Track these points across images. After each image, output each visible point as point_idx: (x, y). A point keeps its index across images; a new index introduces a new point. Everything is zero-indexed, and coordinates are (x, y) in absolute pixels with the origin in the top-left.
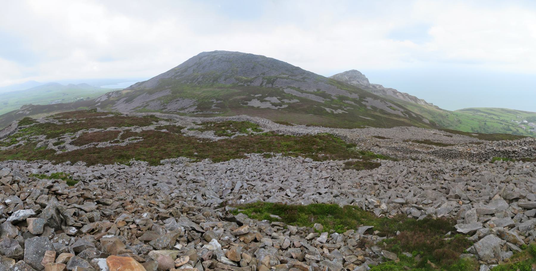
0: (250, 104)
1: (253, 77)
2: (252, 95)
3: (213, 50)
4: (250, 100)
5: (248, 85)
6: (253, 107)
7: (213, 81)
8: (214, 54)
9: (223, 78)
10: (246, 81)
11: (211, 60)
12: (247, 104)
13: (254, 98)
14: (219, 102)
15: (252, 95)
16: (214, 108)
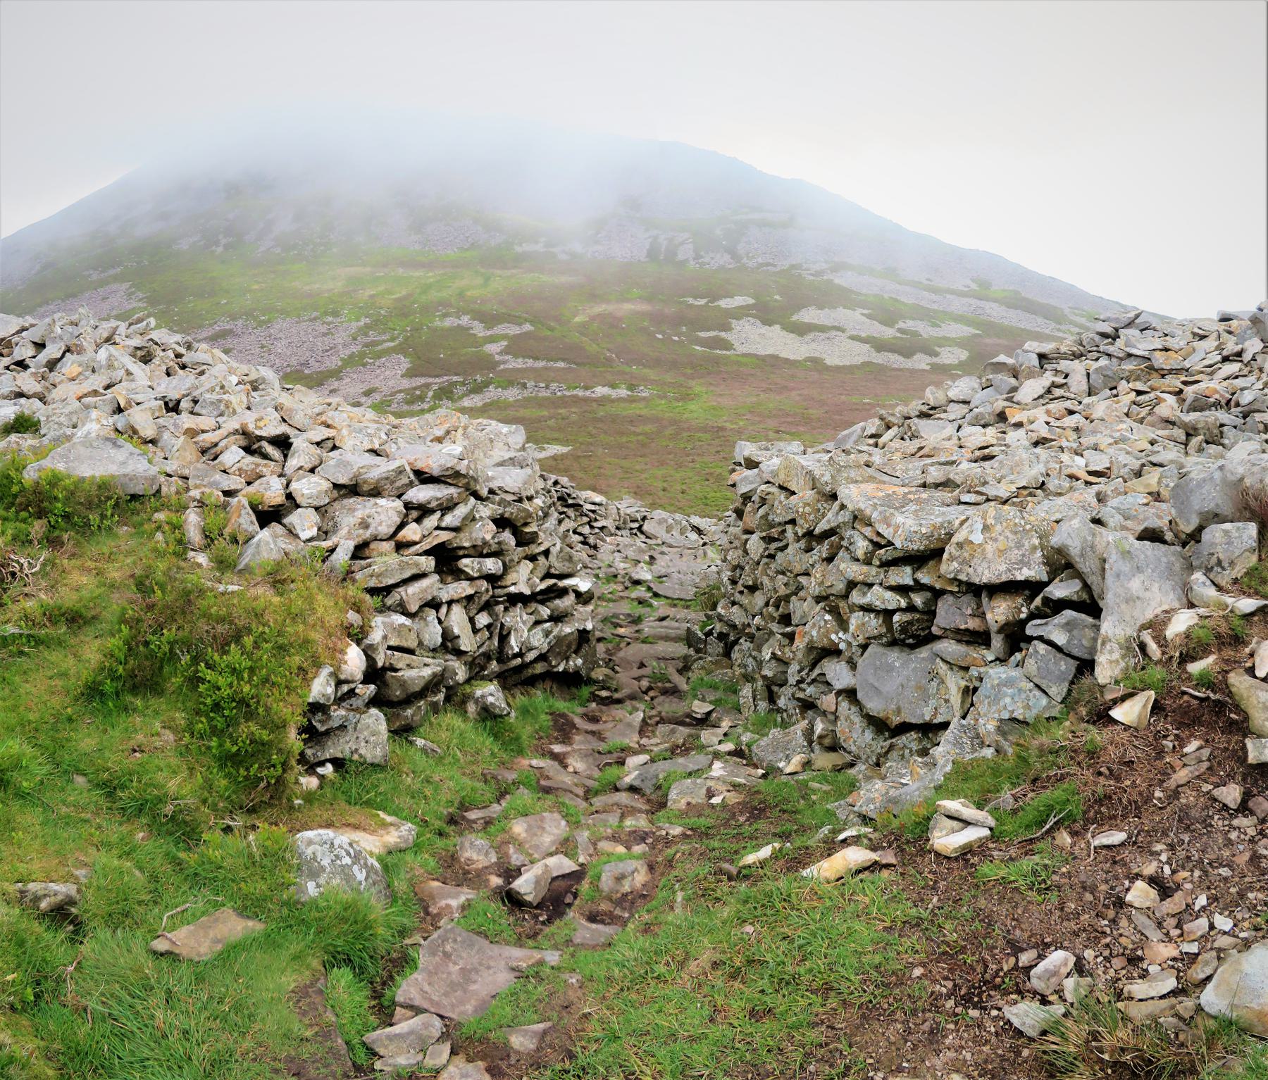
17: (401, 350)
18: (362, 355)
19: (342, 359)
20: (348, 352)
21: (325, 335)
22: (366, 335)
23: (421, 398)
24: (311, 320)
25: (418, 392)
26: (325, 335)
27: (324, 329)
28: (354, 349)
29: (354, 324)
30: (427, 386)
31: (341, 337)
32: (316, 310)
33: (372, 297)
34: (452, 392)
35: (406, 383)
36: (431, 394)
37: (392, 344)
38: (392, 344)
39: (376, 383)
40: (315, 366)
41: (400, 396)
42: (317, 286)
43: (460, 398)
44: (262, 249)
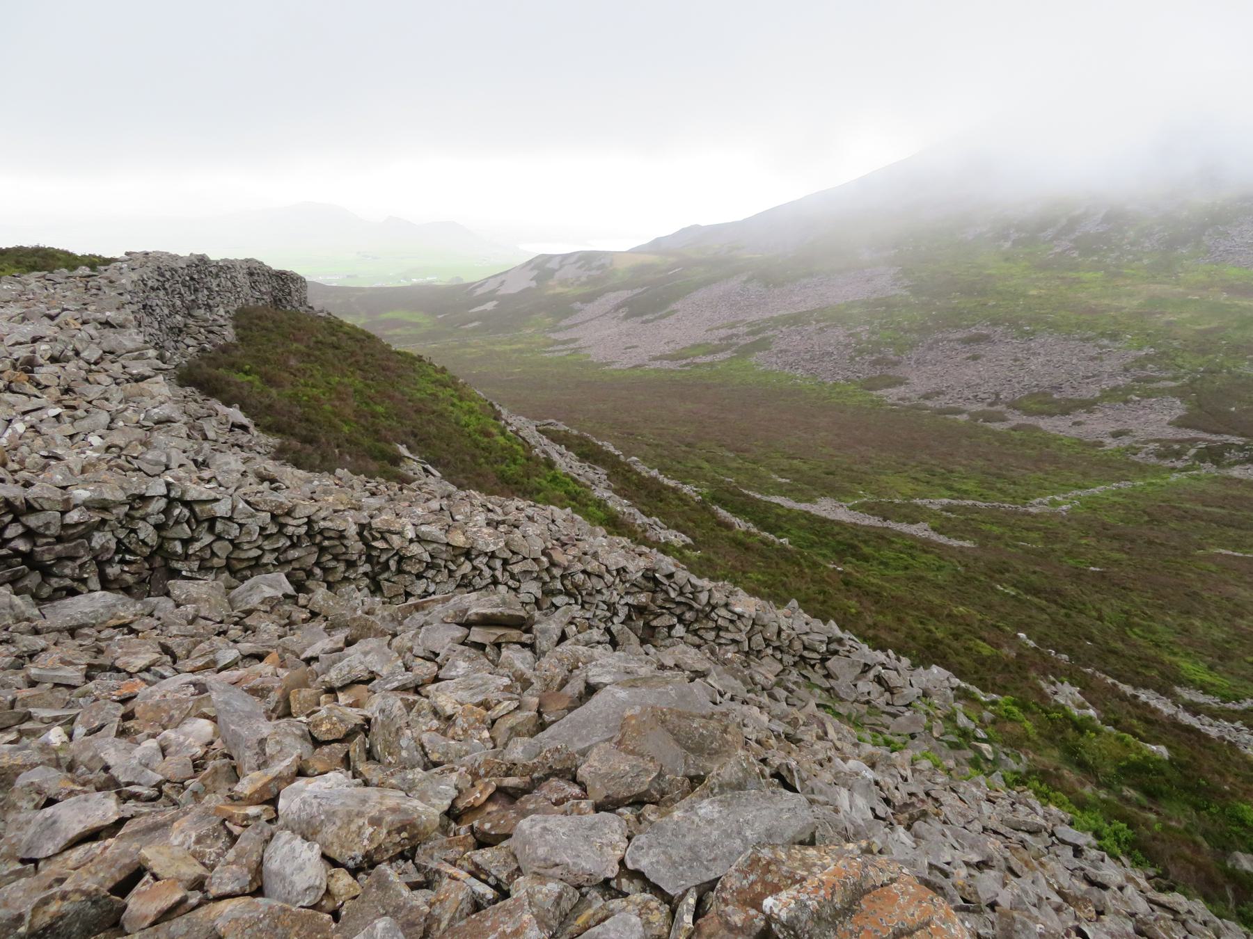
17: (1180, 393)
18: (1129, 390)
19: (1103, 390)
20: (1112, 383)
21: (1092, 359)
22: (1143, 367)
23: (1178, 455)
24: (1081, 340)
25: (1177, 447)
26: (1092, 359)
27: (1094, 353)
28: (1120, 381)
29: (1133, 352)
30: (1193, 441)
31: (1109, 365)
32: (1092, 329)
33: (1169, 323)
34: (1222, 455)
35: (1170, 433)
36: (1193, 451)
37: (1173, 384)
38: (1173, 384)
39: (1133, 425)
40: (1068, 393)
41: (1152, 446)
42: (1106, 302)
43: (1231, 465)
44: (1058, 250)
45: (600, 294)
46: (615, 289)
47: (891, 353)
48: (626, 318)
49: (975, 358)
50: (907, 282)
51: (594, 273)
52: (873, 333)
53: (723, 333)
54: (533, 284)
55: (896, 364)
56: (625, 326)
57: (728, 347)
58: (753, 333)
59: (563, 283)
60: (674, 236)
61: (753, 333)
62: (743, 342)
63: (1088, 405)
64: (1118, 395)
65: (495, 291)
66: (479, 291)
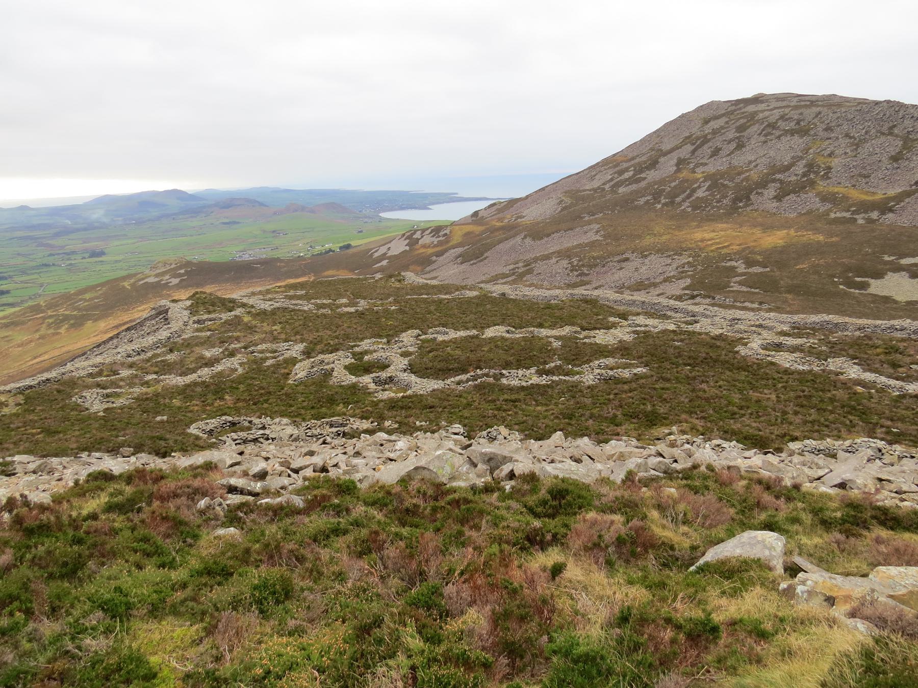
0: (877, 287)
1: (892, 192)
2: (887, 258)
3: (748, 94)
4: (879, 275)
5: (870, 221)
6: (887, 299)
7: (735, 200)
8: (751, 108)
9: (770, 192)
10: (866, 207)
11: (741, 129)
12: (864, 286)
13: (898, 269)
14: (757, 270)
15: (887, 258)
16: (736, 288)
18: (674, 276)
40: (652, 280)
45: (446, 251)
46: (454, 247)
47: (585, 270)
48: (462, 263)
49: (621, 268)
50: (602, 233)
51: (441, 238)
52: (579, 261)
53: (512, 267)
54: (407, 248)
55: (587, 275)
56: (464, 266)
57: (513, 274)
58: (525, 266)
59: (424, 246)
60: (485, 209)
61: (525, 266)
62: (520, 271)
63: (655, 285)
64: (667, 280)
65: (385, 254)
66: (376, 255)
